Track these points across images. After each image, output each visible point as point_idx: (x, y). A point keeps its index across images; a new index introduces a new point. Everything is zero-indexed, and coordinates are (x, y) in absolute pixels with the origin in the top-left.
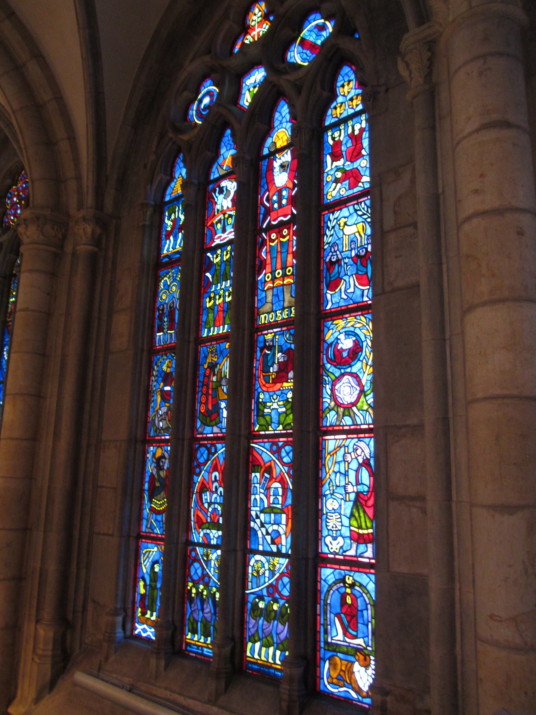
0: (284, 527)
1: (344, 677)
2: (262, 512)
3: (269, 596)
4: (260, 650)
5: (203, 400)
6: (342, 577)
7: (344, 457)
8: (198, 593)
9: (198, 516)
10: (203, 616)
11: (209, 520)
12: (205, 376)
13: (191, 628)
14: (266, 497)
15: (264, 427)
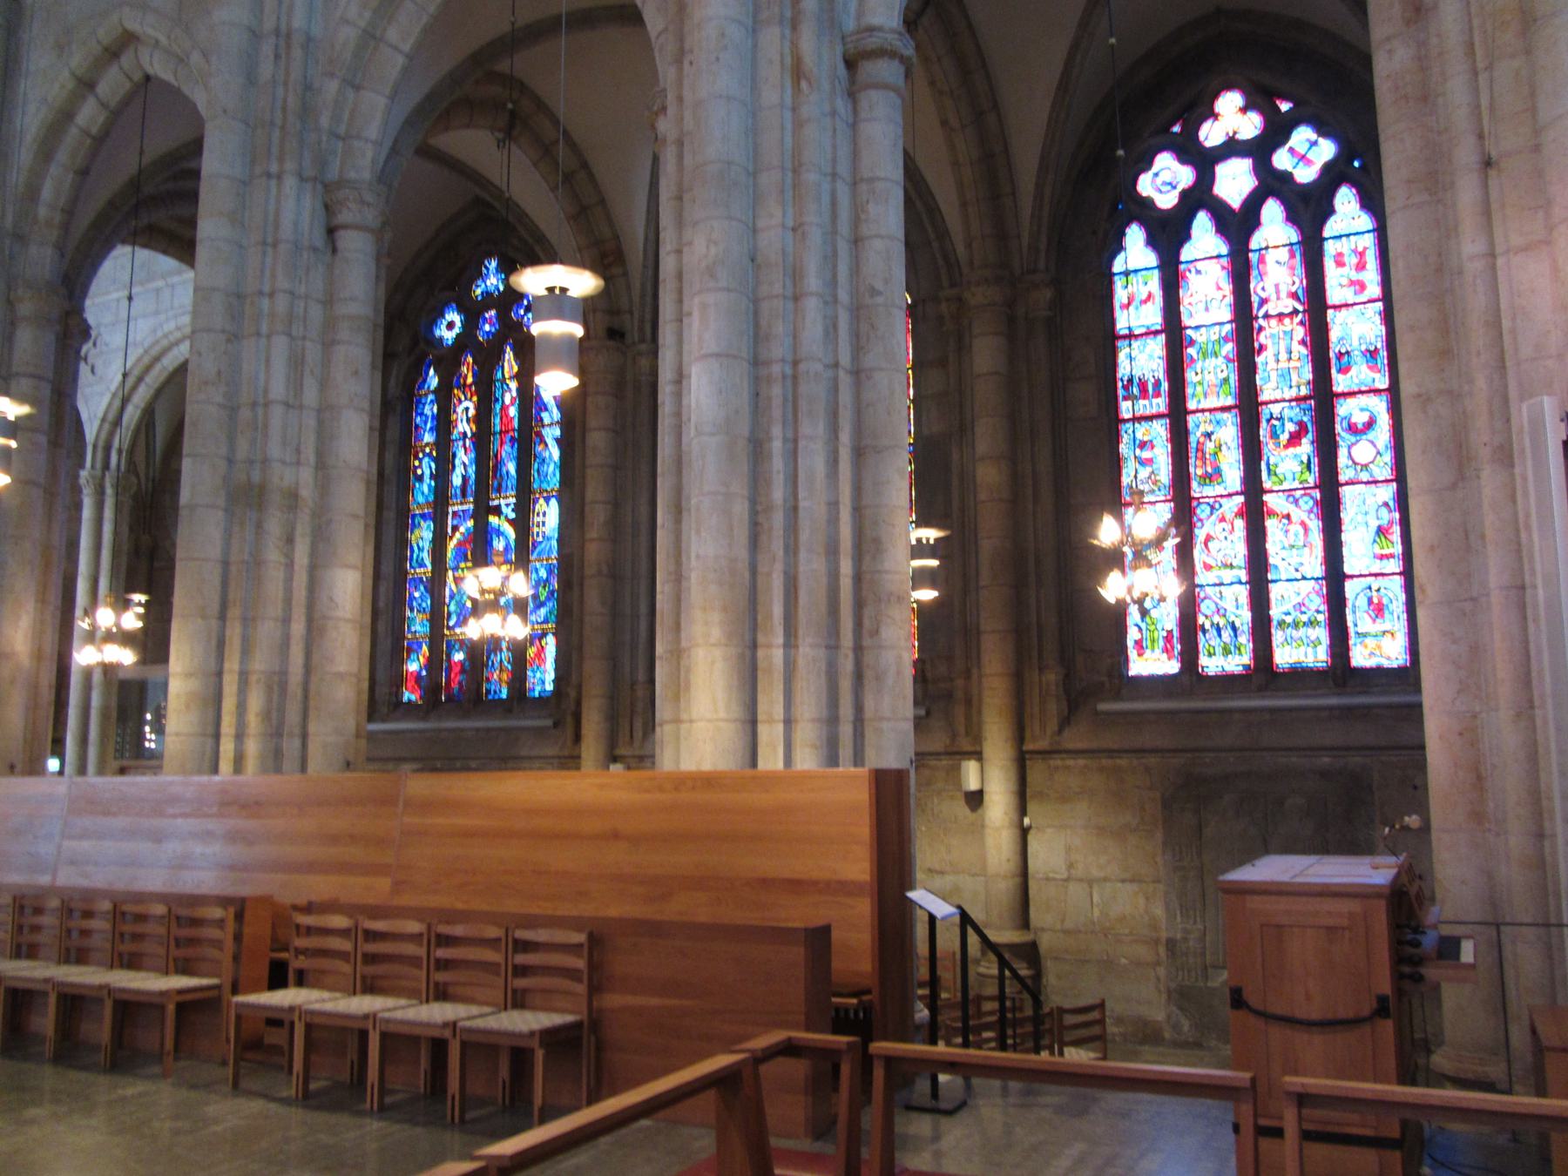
5: (1199, 463)
8: (1212, 625)
9: (1204, 563)
12: (1198, 442)
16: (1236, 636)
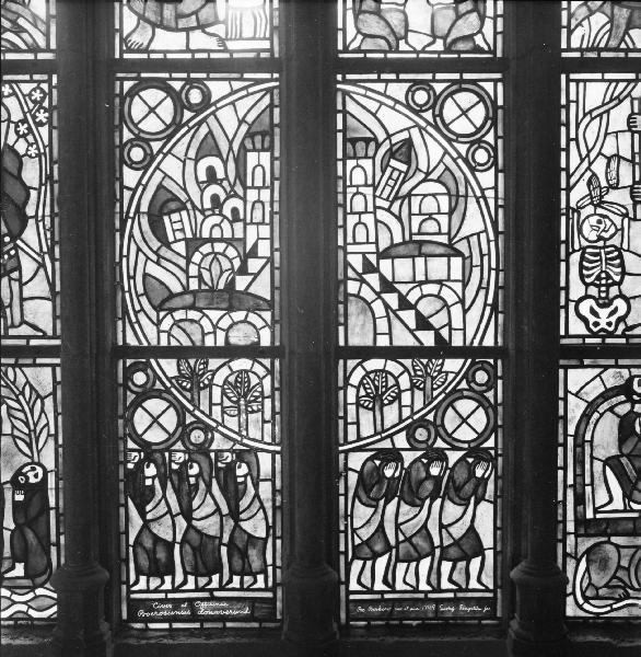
0: (458, 287)
1: (627, 581)
2: (381, 255)
3: (413, 448)
4: (390, 569)
6: (622, 382)
7: (628, 123)
8: (163, 477)
10: (190, 526)
11: (194, 285)
13: (144, 562)
14: (399, 218)
15: (382, 42)
16: (235, 513)
